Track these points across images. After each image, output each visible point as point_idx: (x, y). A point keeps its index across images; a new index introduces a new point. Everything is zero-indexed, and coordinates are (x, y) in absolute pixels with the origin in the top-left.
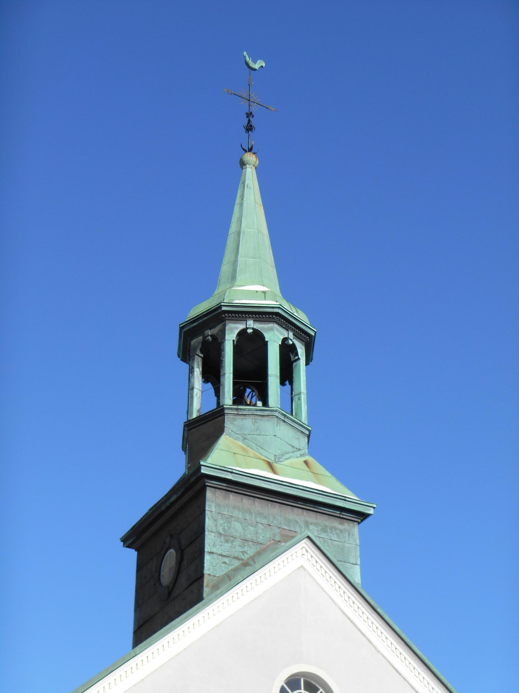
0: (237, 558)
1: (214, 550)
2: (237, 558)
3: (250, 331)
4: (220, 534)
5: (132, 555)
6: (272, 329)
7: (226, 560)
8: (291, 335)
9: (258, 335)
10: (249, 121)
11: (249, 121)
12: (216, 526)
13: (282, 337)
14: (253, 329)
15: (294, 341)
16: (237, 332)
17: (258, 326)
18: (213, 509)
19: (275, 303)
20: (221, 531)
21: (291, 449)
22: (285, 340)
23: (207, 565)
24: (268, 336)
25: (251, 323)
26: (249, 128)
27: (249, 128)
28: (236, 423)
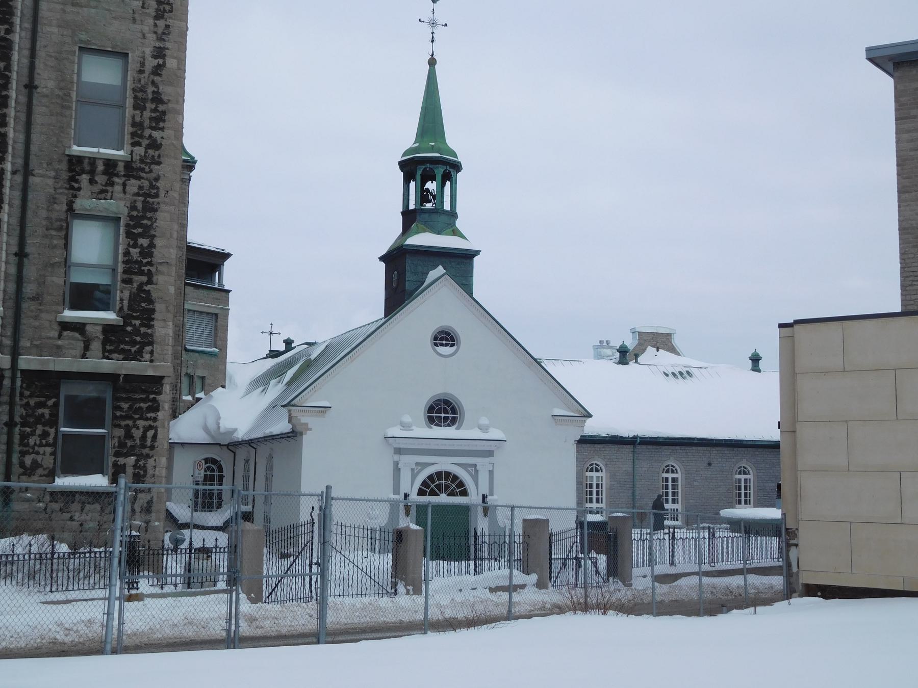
0: (419, 282)
1: (410, 279)
2: (419, 282)
3: (428, 169)
4: (412, 272)
5: (383, 265)
6: (438, 167)
7: (415, 283)
8: (448, 167)
10: (433, 37)
11: (433, 37)
12: (411, 269)
13: (443, 170)
14: (430, 168)
15: (450, 169)
16: (422, 169)
17: (431, 166)
18: (410, 262)
19: (438, 155)
20: (413, 270)
21: (446, 225)
23: (406, 286)
24: (436, 171)
25: (428, 165)
26: (433, 41)
27: (433, 41)
28: (422, 216)
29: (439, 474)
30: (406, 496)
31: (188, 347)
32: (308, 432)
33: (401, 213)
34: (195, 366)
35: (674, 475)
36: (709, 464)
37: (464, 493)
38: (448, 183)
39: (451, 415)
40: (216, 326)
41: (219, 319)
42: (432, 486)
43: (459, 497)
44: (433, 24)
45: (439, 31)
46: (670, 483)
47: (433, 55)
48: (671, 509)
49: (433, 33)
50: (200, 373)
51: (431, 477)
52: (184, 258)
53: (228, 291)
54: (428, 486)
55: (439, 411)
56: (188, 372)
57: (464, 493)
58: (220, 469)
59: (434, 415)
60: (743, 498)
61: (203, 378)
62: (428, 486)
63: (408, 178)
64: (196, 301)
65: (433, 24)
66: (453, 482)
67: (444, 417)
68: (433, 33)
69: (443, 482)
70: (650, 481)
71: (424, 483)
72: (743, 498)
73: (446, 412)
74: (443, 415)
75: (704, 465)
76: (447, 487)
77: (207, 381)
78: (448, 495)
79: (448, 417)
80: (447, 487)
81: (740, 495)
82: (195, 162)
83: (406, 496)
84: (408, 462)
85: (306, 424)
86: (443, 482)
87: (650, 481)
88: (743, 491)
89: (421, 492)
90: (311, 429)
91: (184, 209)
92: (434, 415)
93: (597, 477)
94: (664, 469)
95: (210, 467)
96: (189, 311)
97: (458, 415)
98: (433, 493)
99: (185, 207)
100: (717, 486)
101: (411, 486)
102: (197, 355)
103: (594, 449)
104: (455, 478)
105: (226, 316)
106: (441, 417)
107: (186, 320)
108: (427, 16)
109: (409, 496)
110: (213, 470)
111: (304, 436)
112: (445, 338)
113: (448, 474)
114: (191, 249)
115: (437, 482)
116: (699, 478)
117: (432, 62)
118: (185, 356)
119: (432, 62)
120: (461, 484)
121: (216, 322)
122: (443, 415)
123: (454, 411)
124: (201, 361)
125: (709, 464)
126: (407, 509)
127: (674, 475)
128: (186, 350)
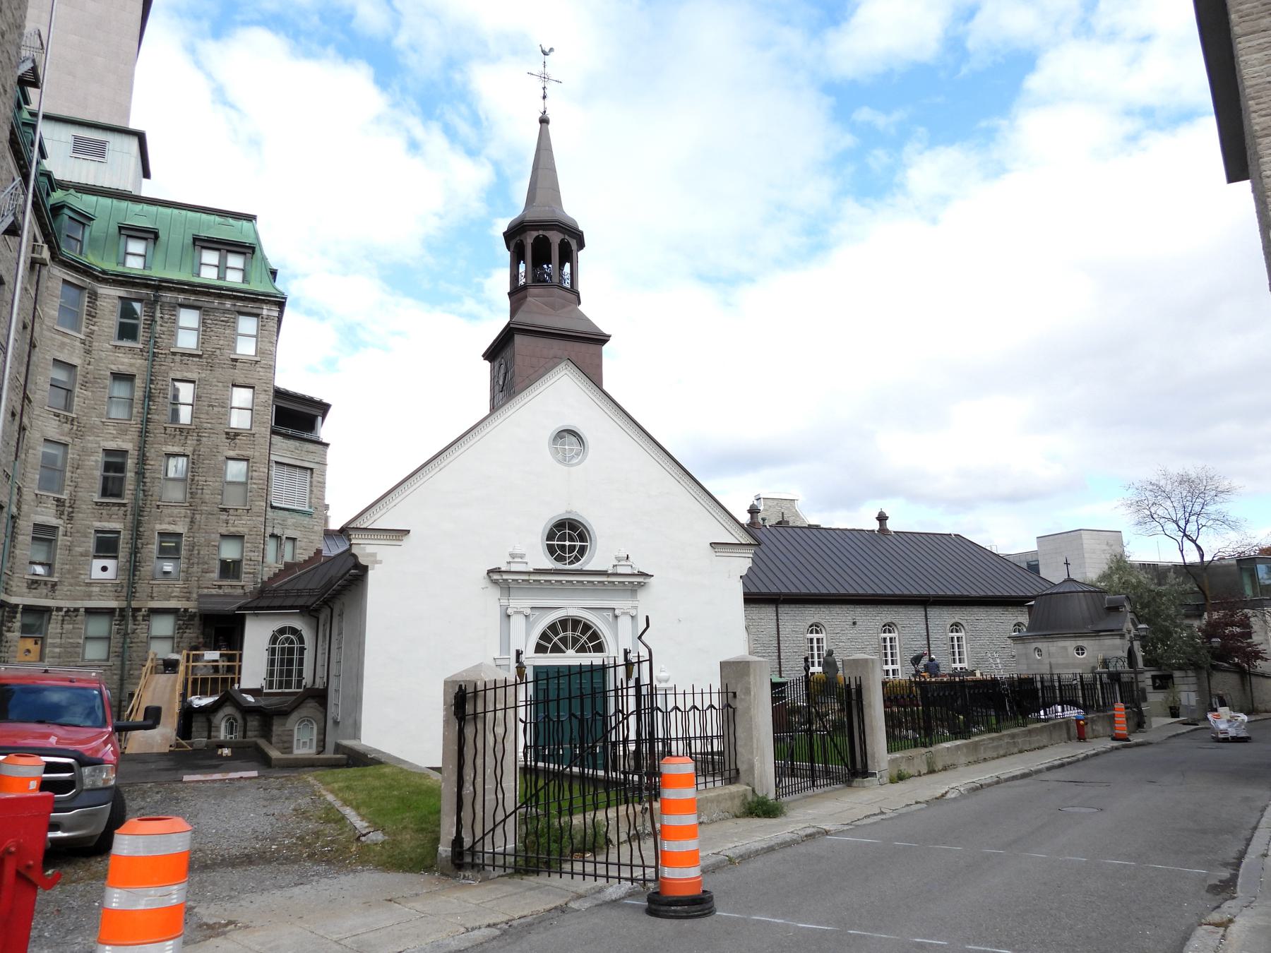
5: (487, 364)
9: (546, 239)
22: (562, 240)
26: (544, 97)
27: (544, 97)
29: (564, 622)
30: (519, 653)
31: (274, 504)
32: (376, 565)
33: (509, 294)
34: (284, 526)
35: (819, 636)
36: (854, 623)
37: (599, 648)
38: (567, 265)
39: (579, 543)
40: (311, 482)
41: (314, 475)
42: (556, 639)
43: (592, 654)
44: (545, 78)
45: (551, 87)
47: (545, 112)
49: (544, 88)
50: (290, 533)
51: (553, 627)
52: (271, 402)
53: (327, 445)
54: (549, 640)
55: (562, 538)
56: (275, 532)
57: (599, 648)
58: (301, 640)
59: (556, 543)
60: (889, 658)
61: (294, 540)
62: (549, 640)
63: (518, 255)
64: (285, 449)
65: (545, 78)
66: (583, 633)
67: (569, 545)
68: (544, 88)
69: (570, 633)
71: (544, 636)
72: (889, 658)
73: (571, 539)
74: (567, 543)
76: (575, 641)
77: (298, 543)
78: (577, 652)
79: (575, 545)
80: (575, 641)
81: (886, 655)
82: (285, 298)
83: (519, 653)
84: (522, 603)
85: (374, 555)
86: (570, 633)
88: (889, 651)
89: (540, 649)
90: (380, 562)
91: (271, 349)
92: (556, 543)
95: (289, 638)
96: (277, 462)
97: (588, 544)
98: (555, 649)
99: (273, 346)
101: (525, 638)
102: (287, 513)
104: (587, 627)
105: (323, 474)
106: (565, 546)
107: (273, 473)
108: (538, 69)
109: (522, 653)
110: (292, 642)
111: (370, 573)
112: (568, 435)
113: (576, 622)
114: (280, 394)
115: (562, 635)
117: (544, 121)
118: (270, 513)
119: (544, 121)
120: (595, 636)
121: (312, 478)
122: (567, 543)
123: (582, 538)
124: (291, 519)
125: (854, 623)
126: (521, 669)
127: (819, 636)
128: (272, 507)
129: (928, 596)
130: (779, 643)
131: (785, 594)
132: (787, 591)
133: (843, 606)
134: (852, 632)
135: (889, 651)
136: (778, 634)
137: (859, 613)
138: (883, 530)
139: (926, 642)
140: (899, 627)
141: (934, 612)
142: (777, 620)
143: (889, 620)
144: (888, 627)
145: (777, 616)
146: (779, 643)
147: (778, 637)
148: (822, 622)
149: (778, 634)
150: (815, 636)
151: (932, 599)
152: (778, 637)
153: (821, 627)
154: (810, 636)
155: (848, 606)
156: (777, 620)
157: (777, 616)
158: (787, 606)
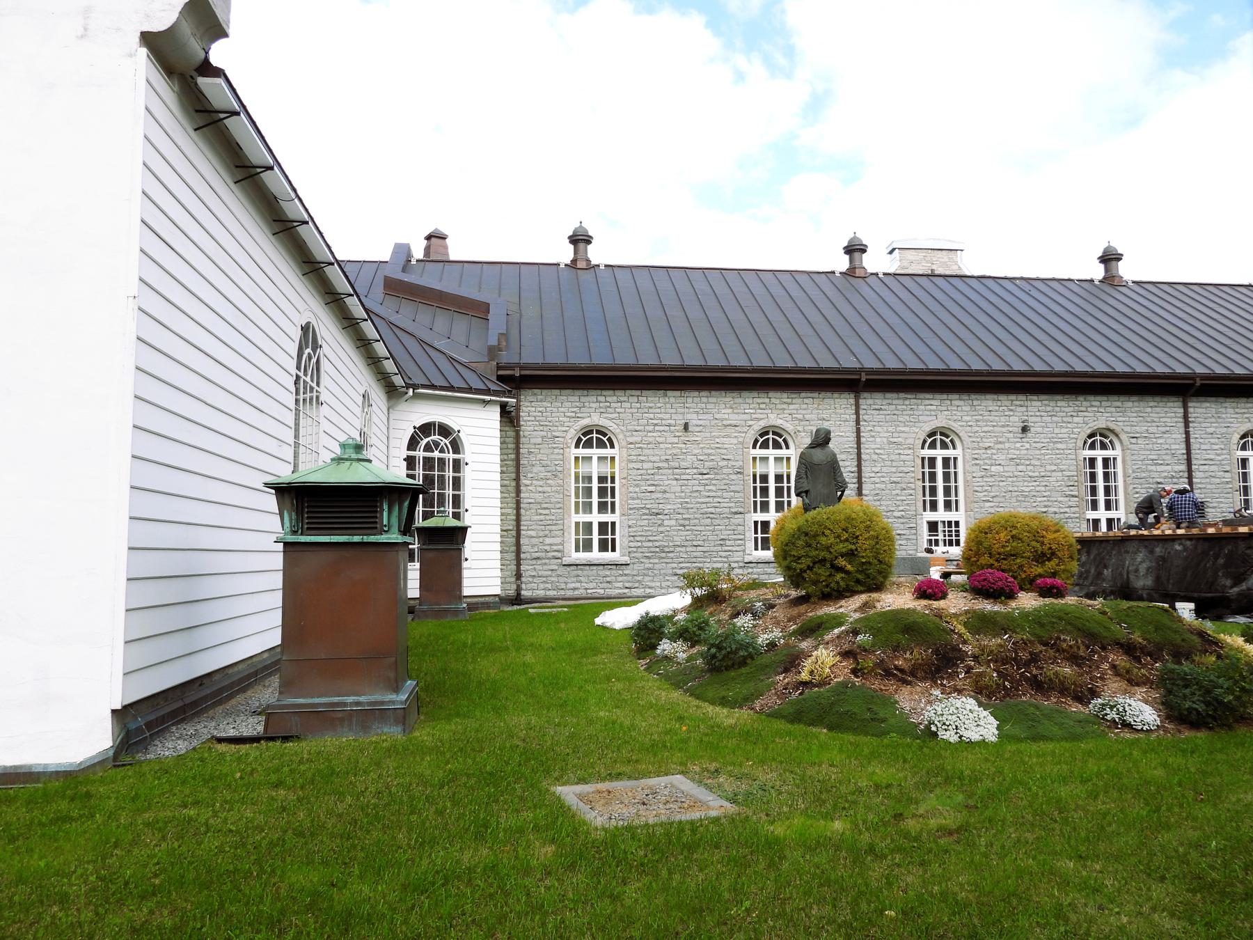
35: (949, 453)
36: (1025, 429)
46: (939, 469)
48: (944, 522)
70: (894, 464)
75: (1015, 429)
81: (1094, 490)
87: (894, 464)
88: (1100, 484)
93: (778, 459)
94: (925, 442)
100: (1043, 474)
103: (767, 400)
116: (1003, 457)
127: (949, 453)
129: (1192, 377)
130: (859, 466)
131: (871, 372)
132: (875, 365)
133: (1003, 397)
134: (1021, 447)
135: (1100, 484)
136: (859, 448)
137: (1036, 410)
138: (1111, 279)
139: (1184, 467)
140: (1123, 437)
141: (1202, 410)
142: (858, 422)
143: (1101, 424)
144: (1099, 438)
145: (857, 413)
146: (859, 466)
147: (859, 454)
148: (955, 426)
149: (859, 448)
150: (939, 453)
151: (1198, 383)
152: (859, 454)
153: (953, 436)
154: (928, 453)
155: (1013, 397)
156: (858, 422)
157: (857, 413)
158: (879, 395)
